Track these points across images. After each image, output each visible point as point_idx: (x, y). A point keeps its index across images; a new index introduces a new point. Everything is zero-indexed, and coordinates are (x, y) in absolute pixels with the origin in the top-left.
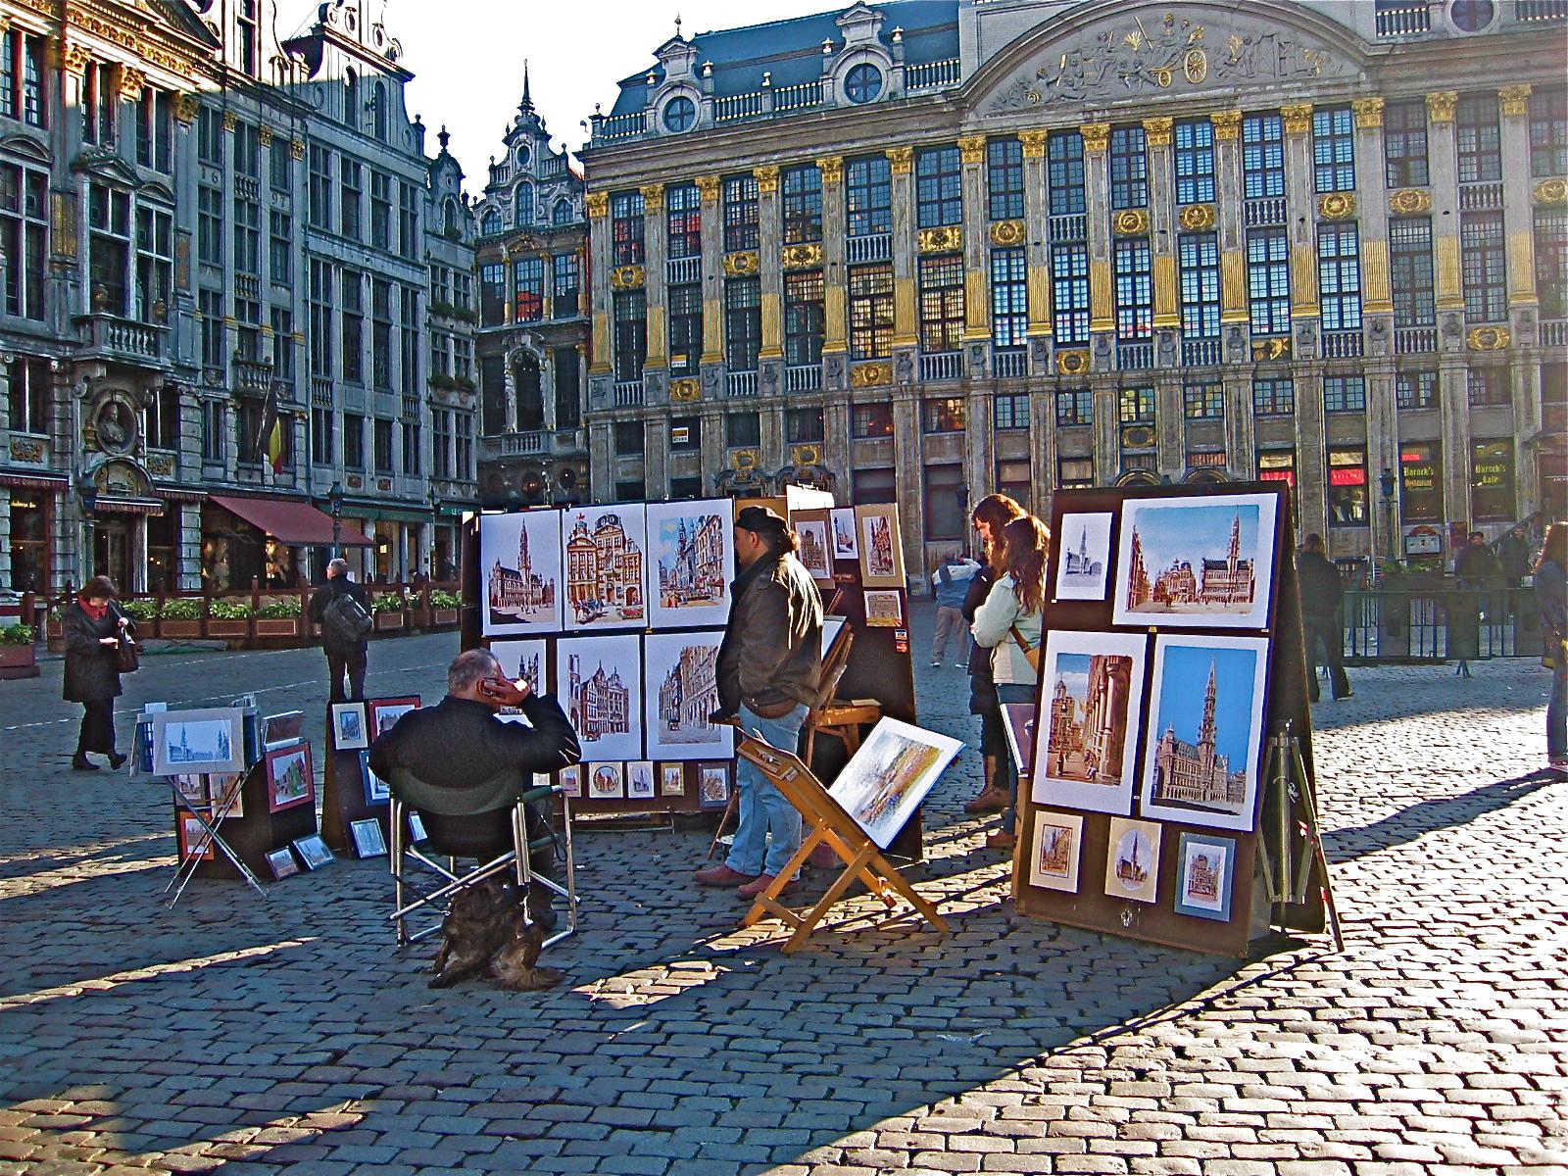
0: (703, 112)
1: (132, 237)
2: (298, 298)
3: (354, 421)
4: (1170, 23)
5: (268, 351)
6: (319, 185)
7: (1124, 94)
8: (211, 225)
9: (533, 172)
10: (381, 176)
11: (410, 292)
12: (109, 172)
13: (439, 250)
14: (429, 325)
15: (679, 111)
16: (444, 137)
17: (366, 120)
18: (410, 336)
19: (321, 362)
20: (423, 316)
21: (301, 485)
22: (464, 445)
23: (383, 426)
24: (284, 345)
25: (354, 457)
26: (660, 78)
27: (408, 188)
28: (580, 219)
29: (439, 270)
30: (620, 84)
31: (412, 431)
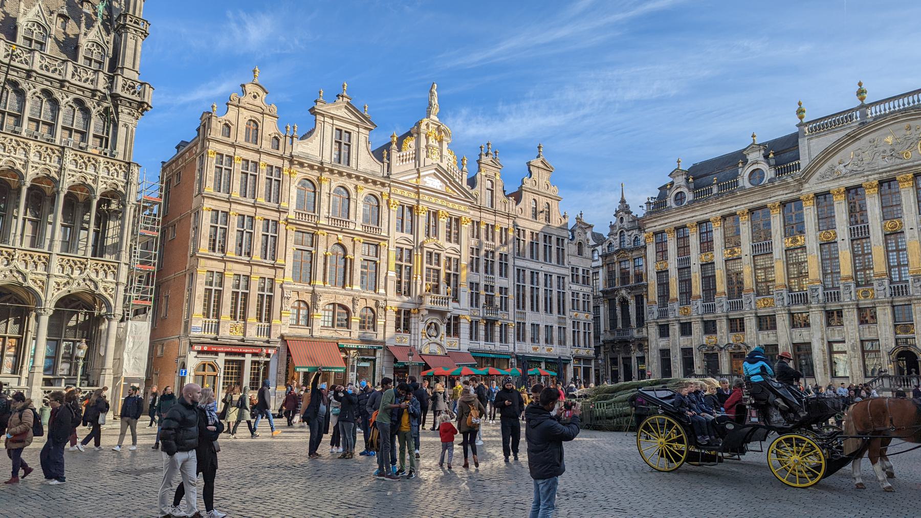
1: (442, 268)
4: (909, 128)
7: (884, 164)
13: (575, 261)
15: (679, 198)
28: (643, 243)
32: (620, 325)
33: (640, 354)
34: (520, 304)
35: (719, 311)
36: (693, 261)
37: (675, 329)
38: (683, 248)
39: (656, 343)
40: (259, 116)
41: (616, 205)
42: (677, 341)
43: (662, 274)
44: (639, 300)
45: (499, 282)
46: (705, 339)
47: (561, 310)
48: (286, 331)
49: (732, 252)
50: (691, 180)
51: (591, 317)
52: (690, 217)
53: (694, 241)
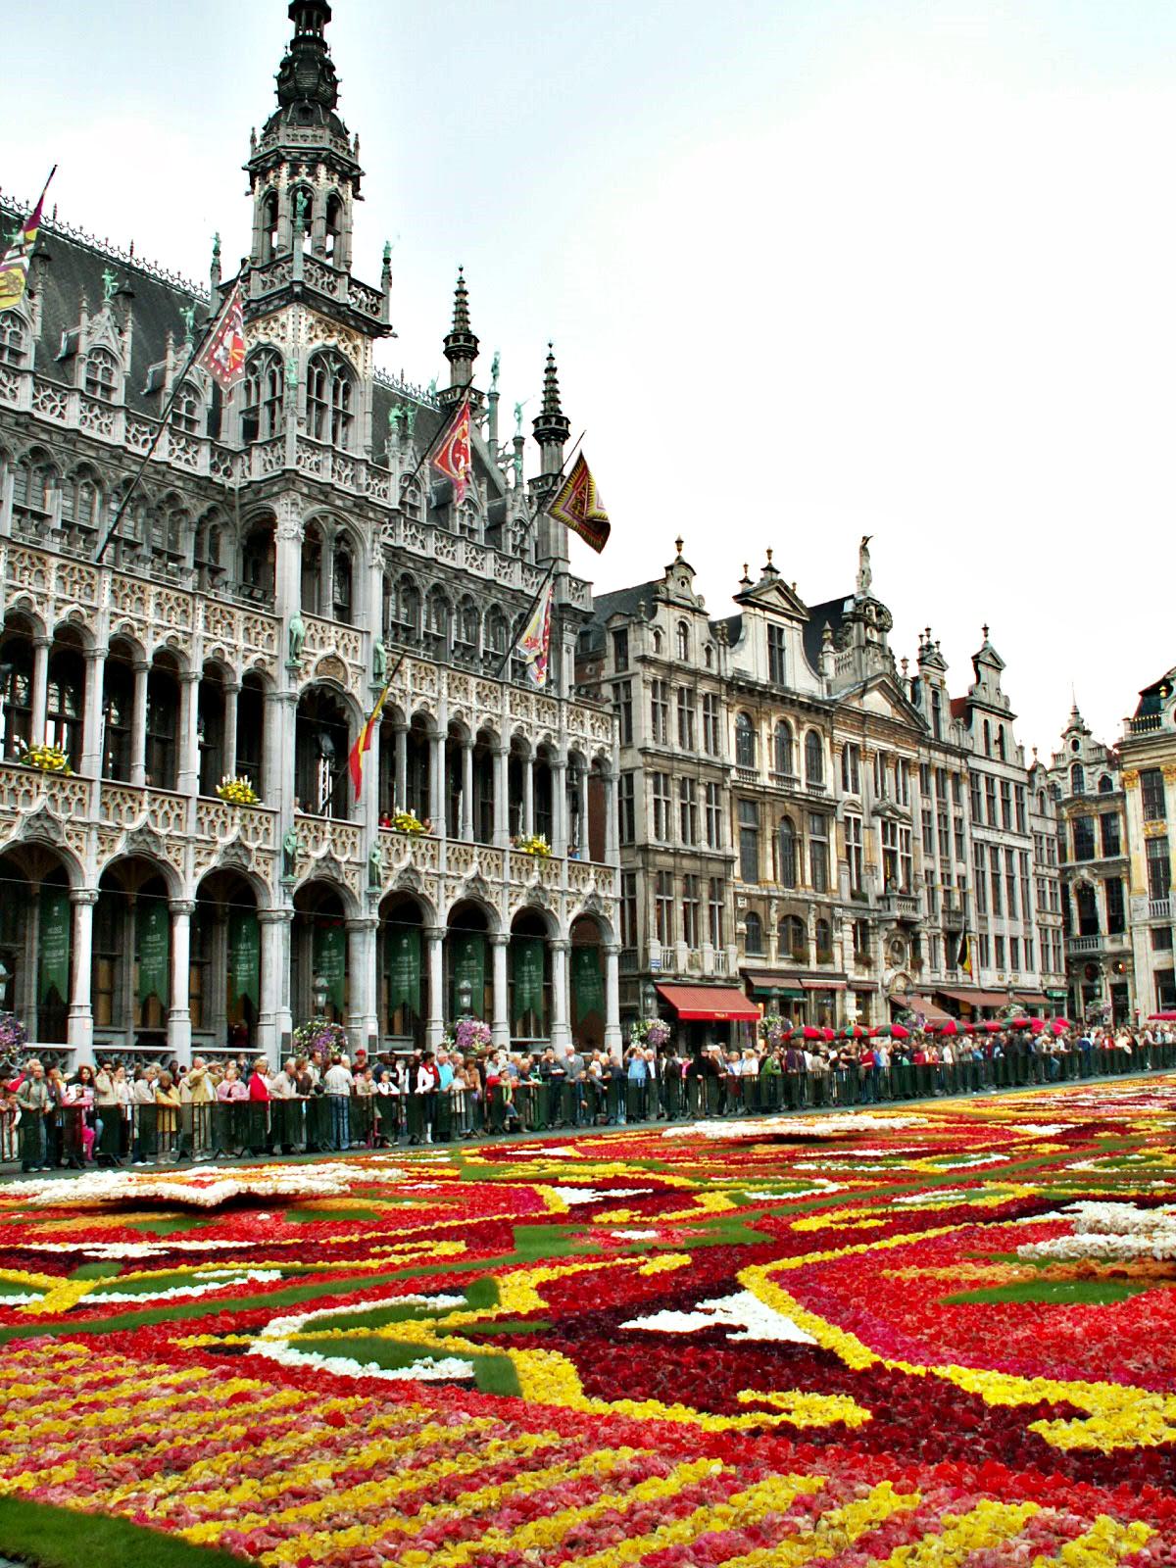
1: (898, 848)
2: (966, 868)
3: (999, 939)
6: (975, 796)
8: (927, 831)
9: (1083, 758)
10: (1005, 784)
11: (1023, 854)
12: (888, 814)
14: (1035, 874)
17: (995, 750)
18: (1025, 881)
20: (1031, 868)
21: (975, 981)
22: (1056, 948)
23: (1014, 940)
24: (964, 896)
25: (1000, 964)
27: (1019, 789)
28: (1117, 789)
29: (1038, 837)
30: (1141, 693)
31: (1028, 942)
33: (1117, 979)
34: (981, 906)
40: (689, 616)
44: (1114, 888)
48: (744, 963)
51: (1060, 920)
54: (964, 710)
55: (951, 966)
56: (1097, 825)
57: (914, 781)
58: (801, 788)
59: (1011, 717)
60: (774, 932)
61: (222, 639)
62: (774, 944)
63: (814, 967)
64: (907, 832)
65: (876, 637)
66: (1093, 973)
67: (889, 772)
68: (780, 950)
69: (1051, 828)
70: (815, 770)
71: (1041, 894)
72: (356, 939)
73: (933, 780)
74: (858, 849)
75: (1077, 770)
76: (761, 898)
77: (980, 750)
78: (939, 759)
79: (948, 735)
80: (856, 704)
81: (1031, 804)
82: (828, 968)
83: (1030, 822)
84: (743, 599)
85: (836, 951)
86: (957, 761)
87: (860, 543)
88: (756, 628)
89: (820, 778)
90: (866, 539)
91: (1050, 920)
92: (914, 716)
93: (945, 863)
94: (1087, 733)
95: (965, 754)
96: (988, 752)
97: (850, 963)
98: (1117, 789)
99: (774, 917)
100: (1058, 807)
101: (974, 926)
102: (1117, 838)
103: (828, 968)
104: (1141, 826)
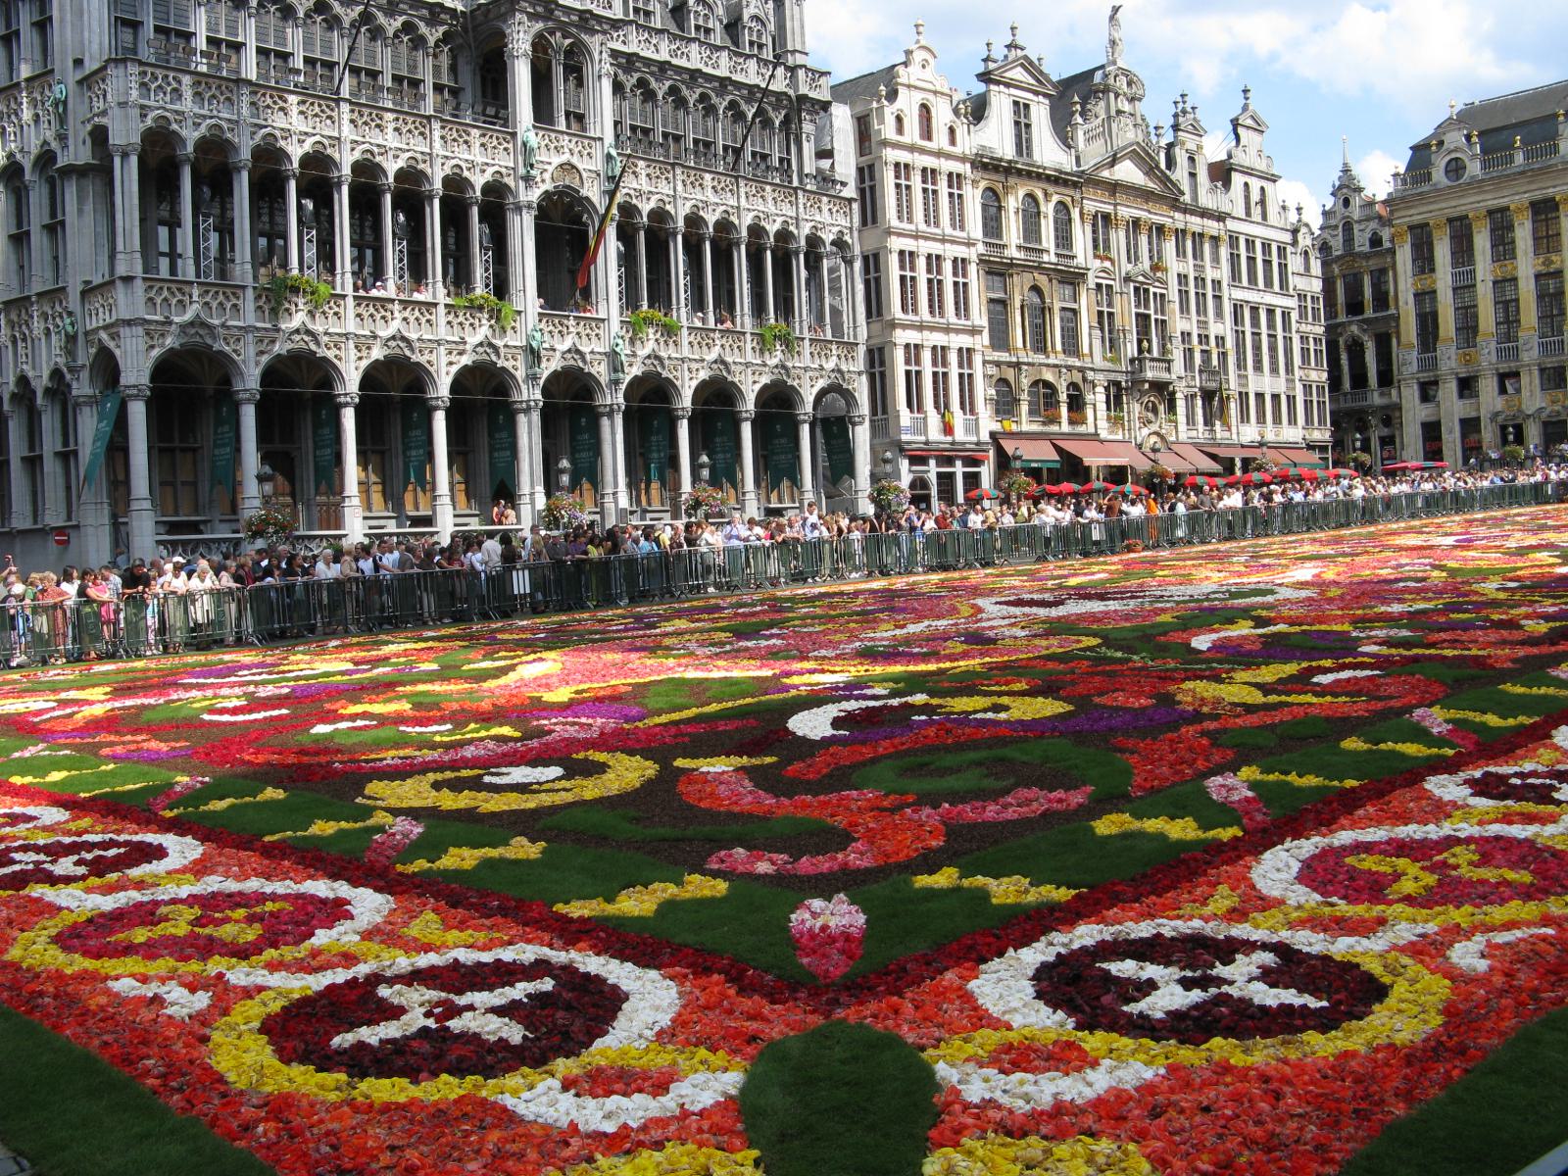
0: (1474, 168)
3: (1260, 396)
5: (1215, 362)
6: (1234, 259)
8: (1183, 295)
11: (1286, 315)
15: (1455, 168)
16: (1299, 209)
17: (1256, 212)
19: (1241, 364)
23: (1276, 397)
24: (1223, 355)
25: (1261, 419)
26: (1441, 143)
27: (1282, 251)
29: (1302, 297)
31: (1291, 399)
32: (1347, 385)
33: (1385, 432)
35: (1525, 357)
36: (1479, 276)
37: (1449, 390)
38: (1463, 251)
39: (1414, 413)
40: (931, 97)
41: (1334, 177)
42: (1452, 407)
43: (1425, 297)
45: (1215, 329)
46: (1499, 403)
47: (1289, 369)
49: (1548, 262)
50: (1475, 139)
52: (1473, 204)
53: (1482, 241)
54: (1222, 173)
55: (1209, 422)
56: (1367, 281)
57: (1169, 246)
58: (1050, 258)
59: (1273, 179)
60: (1025, 396)
61: (462, 154)
62: (1024, 408)
63: (1065, 427)
64: (1162, 296)
65: (1126, 107)
66: (1363, 427)
67: (1143, 239)
68: (1031, 413)
69: (1317, 286)
70: (1064, 238)
71: (1305, 352)
72: (605, 422)
73: (1189, 244)
74: (1111, 315)
75: (1348, 227)
76: (1010, 364)
77: (1240, 212)
78: (1195, 223)
79: (1206, 200)
80: (1105, 174)
81: (1295, 263)
82: (1081, 429)
83: (1293, 281)
84: (985, 77)
85: (1089, 412)
86: (1215, 224)
87: (1109, 12)
88: (1001, 104)
89: (1070, 246)
90: (1116, 10)
91: (1314, 375)
92: (1165, 180)
93: (1202, 324)
94: (1359, 190)
95: (1221, 217)
96: (1248, 213)
97: (1103, 424)
98: (1387, 245)
99: (1025, 382)
100: (1325, 264)
101: (1233, 384)
102: (1387, 293)
103: (1081, 429)
104: (1410, 281)
